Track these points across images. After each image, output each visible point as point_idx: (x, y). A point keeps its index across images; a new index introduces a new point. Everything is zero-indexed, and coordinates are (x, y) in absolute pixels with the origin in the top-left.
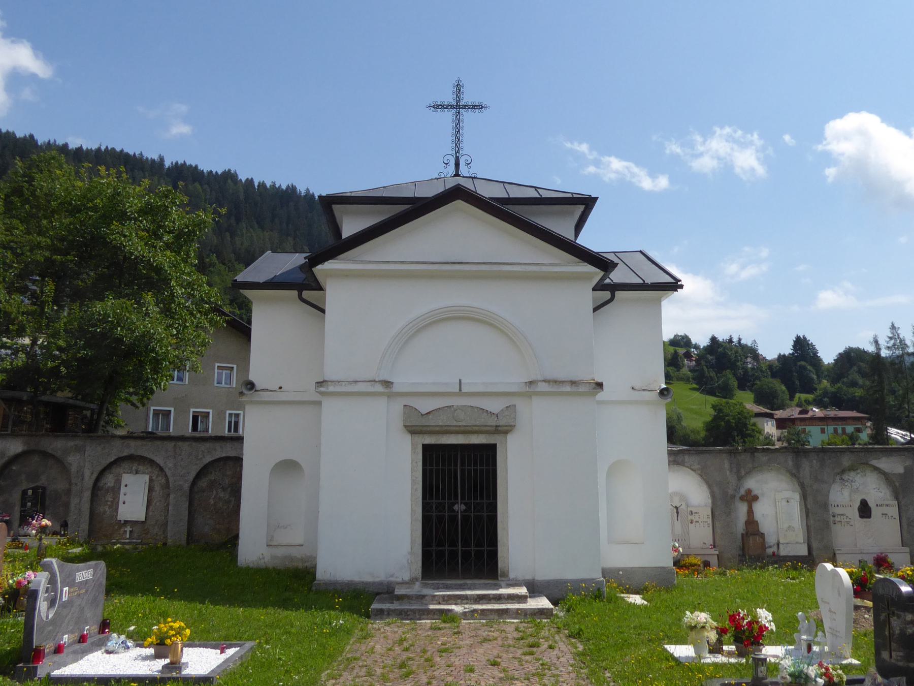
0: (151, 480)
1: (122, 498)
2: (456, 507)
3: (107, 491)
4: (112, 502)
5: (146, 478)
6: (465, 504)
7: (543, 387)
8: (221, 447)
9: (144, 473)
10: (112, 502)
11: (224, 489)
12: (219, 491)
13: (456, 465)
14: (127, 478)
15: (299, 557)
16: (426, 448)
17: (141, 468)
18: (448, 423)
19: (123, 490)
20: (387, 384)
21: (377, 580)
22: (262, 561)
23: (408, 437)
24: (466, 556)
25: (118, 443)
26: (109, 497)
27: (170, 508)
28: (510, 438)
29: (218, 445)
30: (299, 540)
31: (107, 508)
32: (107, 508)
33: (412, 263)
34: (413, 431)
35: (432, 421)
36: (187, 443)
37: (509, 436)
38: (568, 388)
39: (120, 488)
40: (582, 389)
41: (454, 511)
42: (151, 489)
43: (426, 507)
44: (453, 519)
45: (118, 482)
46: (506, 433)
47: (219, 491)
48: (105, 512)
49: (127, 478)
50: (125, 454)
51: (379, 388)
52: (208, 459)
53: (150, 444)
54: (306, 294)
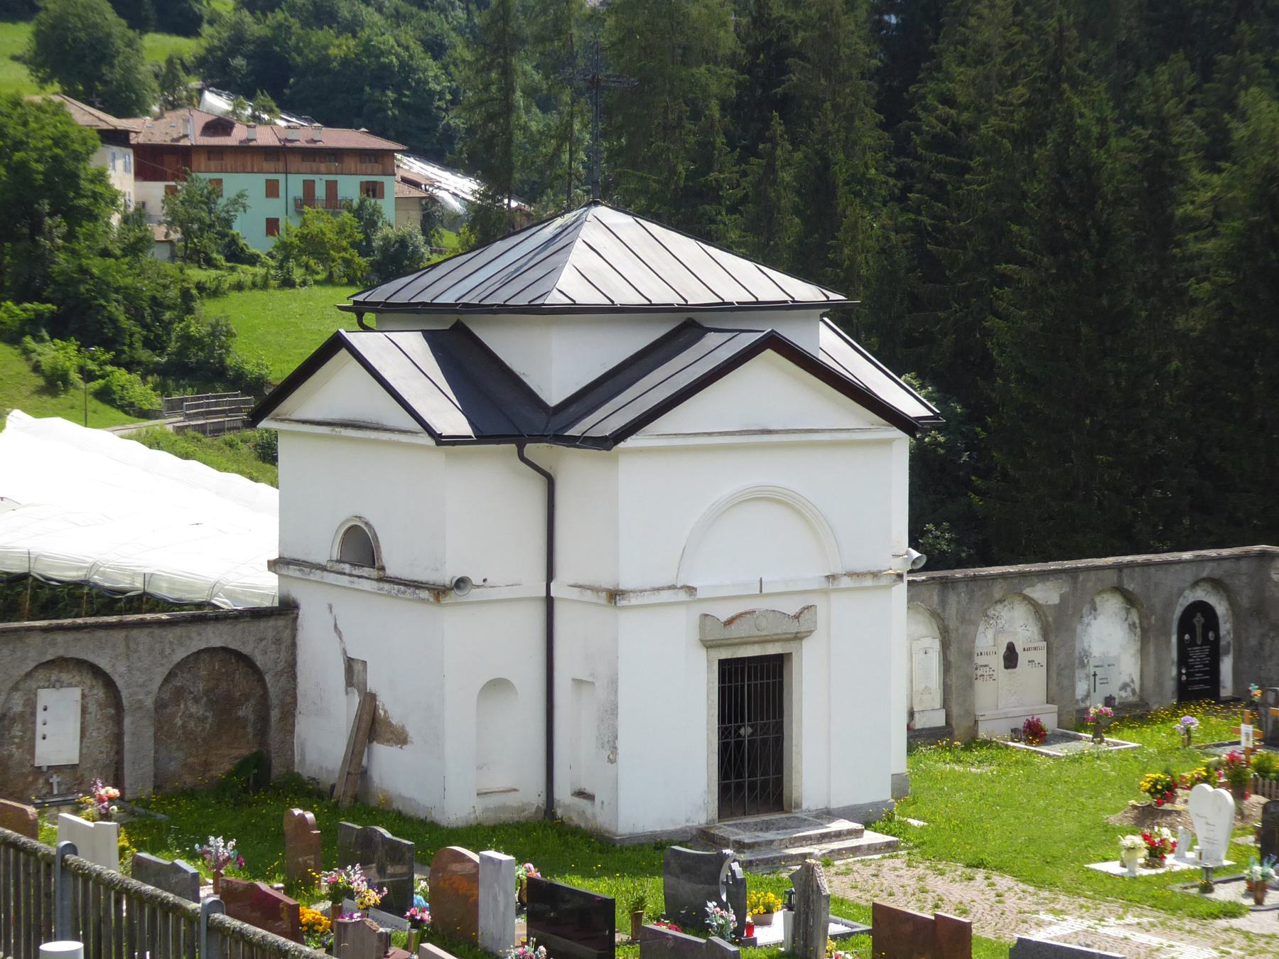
0: (84, 696)
1: (40, 729)
2: (742, 731)
3: (13, 721)
4: (22, 738)
5: (76, 693)
6: (752, 726)
7: (846, 582)
8: (199, 634)
9: (70, 685)
10: (22, 738)
11: (196, 700)
12: (190, 703)
13: (743, 680)
14: (46, 696)
15: (515, 805)
16: (722, 663)
17: (65, 677)
18: (752, 633)
19: (40, 716)
20: (691, 590)
21: (678, 827)
22: (472, 816)
23: (703, 652)
24: (752, 787)
25: (37, 639)
26: (17, 730)
27: (126, 739)
28: (806, 644)
29: (194, 629)
30: (1252, 838)
31: (14, 749)
32: (14, 749)
33: (721, 434)
34: (709, 645)
35: (737, 631)
36: (146, 631)
37: (804, 642)
38: (869, 582)
39: (33, 714)
40: (883, 582)
41: (740, 736)
42: (84, 711)
43: (724, 733)
44: (739, 744)
45: (31, 705)
46: (801, 639)
47: (190, 703)
48: (11, 756)
49: (46, 696)
50: (49, 657)
51: (683, 596)
52: (180, 654)
53: (86, 636)
54: (532, 449)
